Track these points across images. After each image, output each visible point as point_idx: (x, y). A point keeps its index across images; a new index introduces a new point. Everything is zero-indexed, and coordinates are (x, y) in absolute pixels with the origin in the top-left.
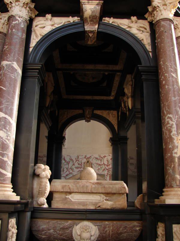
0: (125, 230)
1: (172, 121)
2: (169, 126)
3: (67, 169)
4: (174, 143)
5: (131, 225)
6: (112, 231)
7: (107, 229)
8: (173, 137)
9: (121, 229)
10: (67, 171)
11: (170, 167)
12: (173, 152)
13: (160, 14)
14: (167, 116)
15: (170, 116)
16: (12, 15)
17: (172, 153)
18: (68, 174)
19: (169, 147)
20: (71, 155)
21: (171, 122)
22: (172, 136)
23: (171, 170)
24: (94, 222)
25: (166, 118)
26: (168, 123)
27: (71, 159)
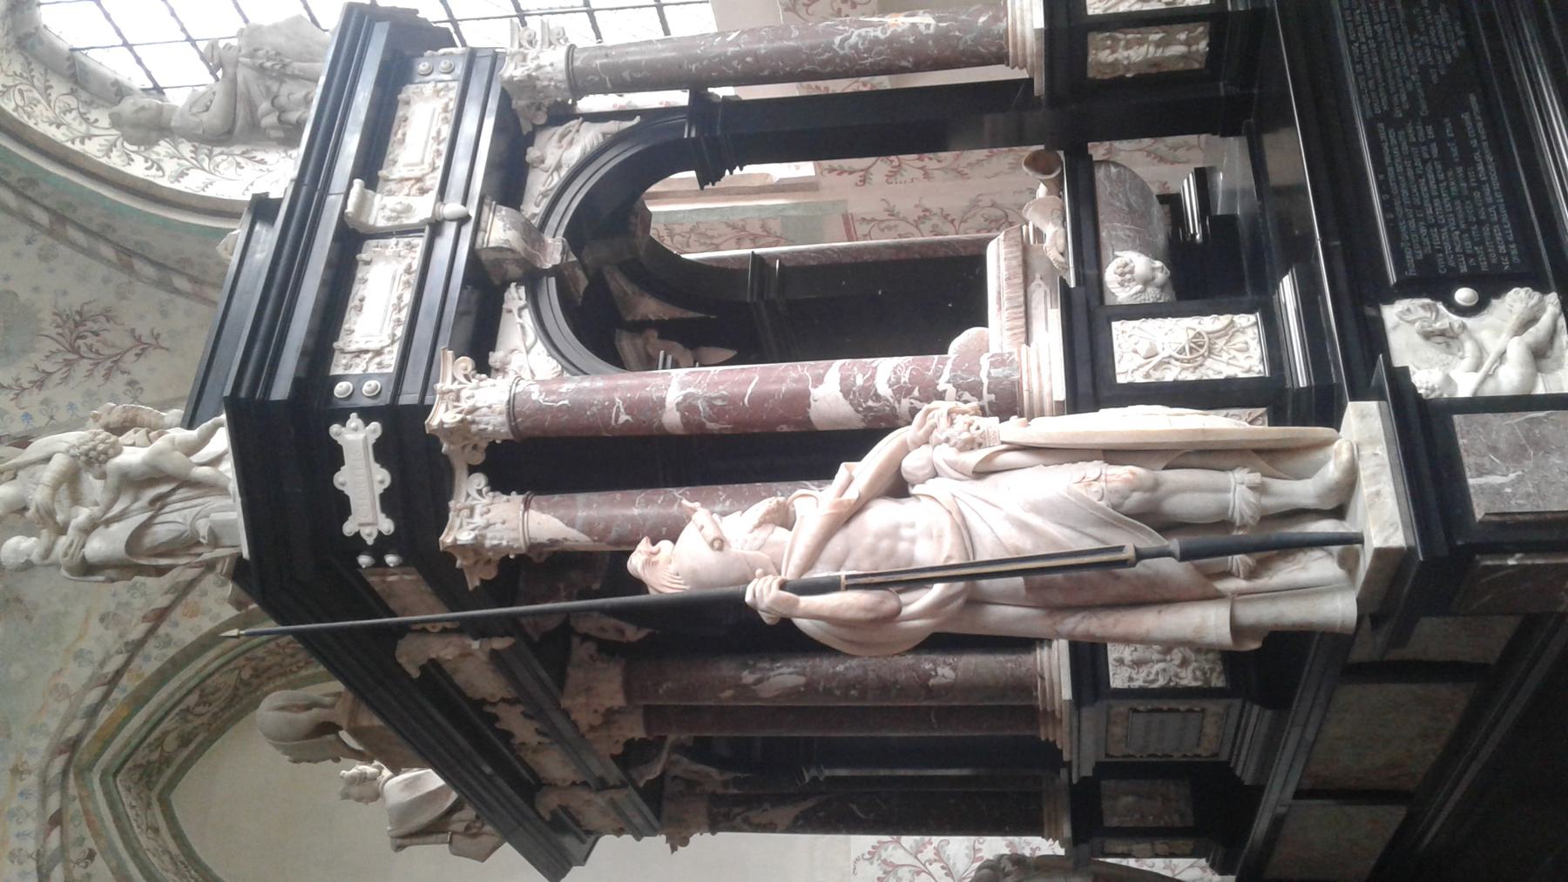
0: (1120, 195)
1: (850, 36)
2: (863, 44)
3: (918, 873)
4: (904, 30)
5: (1107, 183)
6: (1126, 223)
7: (1121, 233)
8: (889, 33)
9: (1118, 204)
10: (930, 874)
11: (959, 38)
12: (925, 32)
13: (549, 69)
14: (838, 49)
15: (837, 40)
16: (509, 401)
17: (927, 35)
18: (943, 868)
19: (912, 42)
20: (853, 857)
21: (853, 40)
22: (888, 35)
23: (968, 37)
24: (1104, 261)
25: (841, 52)
26: (855, 47)
27: (869, 853)
